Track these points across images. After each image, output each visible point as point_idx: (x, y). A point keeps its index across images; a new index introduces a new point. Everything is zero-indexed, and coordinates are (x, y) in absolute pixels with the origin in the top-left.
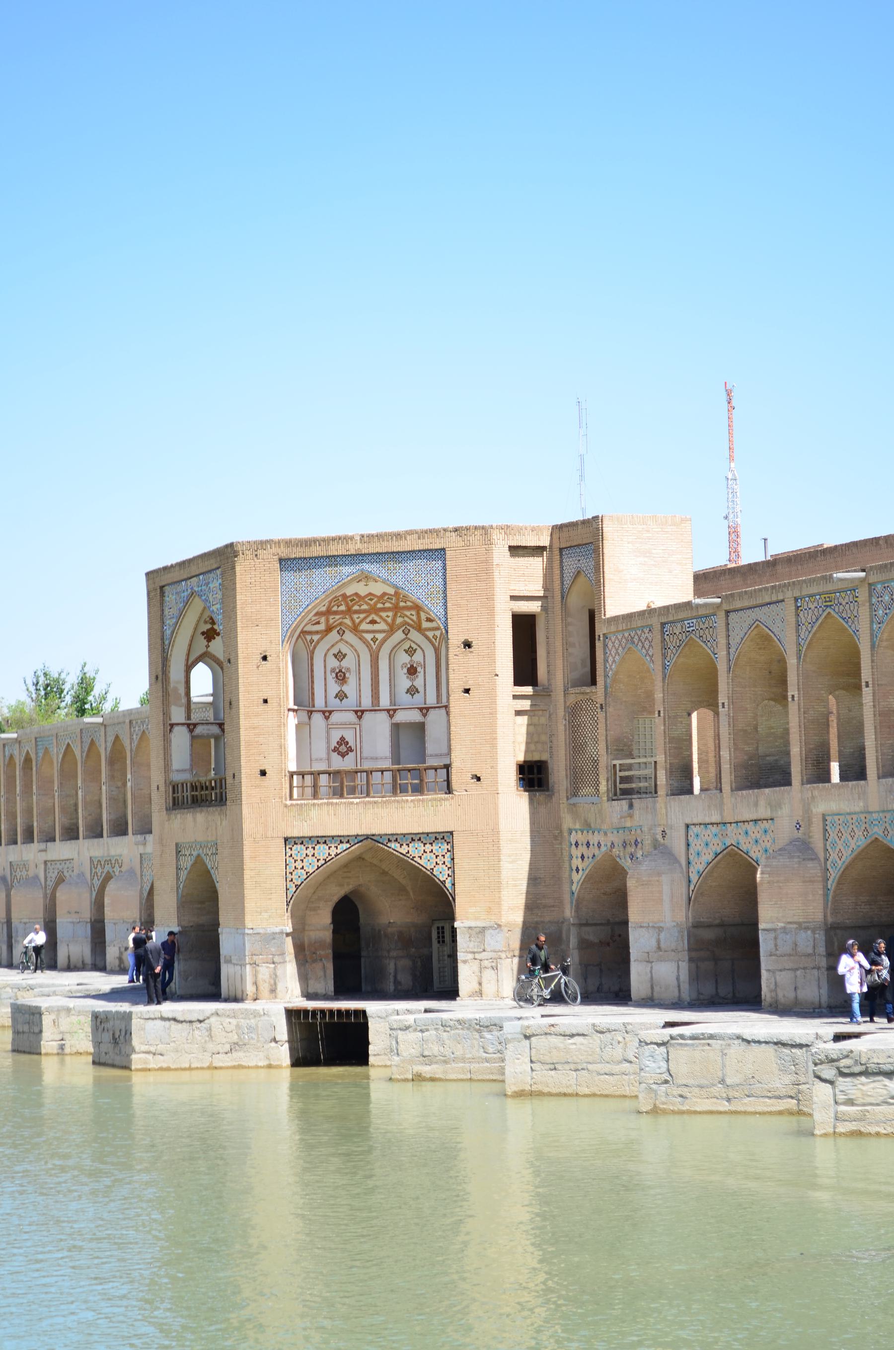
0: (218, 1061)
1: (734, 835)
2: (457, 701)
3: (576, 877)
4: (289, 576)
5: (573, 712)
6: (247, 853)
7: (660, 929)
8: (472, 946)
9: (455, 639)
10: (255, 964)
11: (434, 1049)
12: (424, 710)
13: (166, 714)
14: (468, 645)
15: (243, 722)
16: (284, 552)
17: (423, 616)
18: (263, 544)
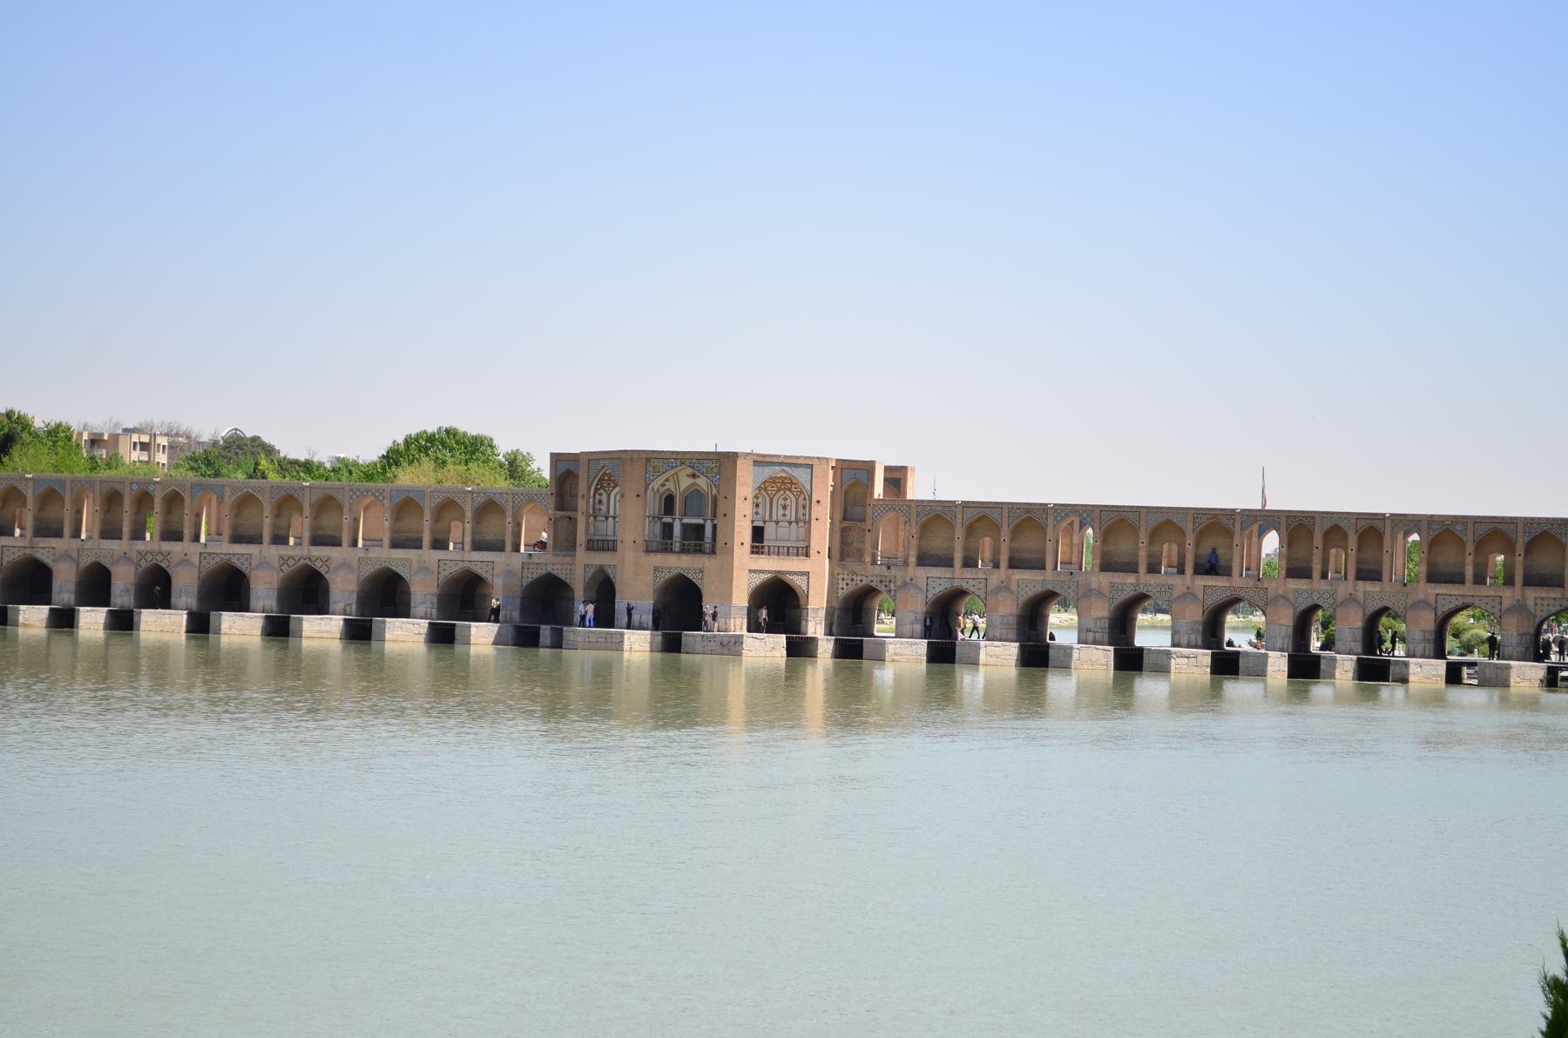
0: (769, 654)
1: (957, 583)
2: (813, 522)
3: (840, 591)
4: (757, 468)
5: (844, 531)
6: (734, 575)
7: (917, 613)
8: (814, 615)
9: (814, 499)
10: (735, 618)
11: (898, 651)
12: (765, 522)
13: (645, 512)
14: (818, 502)
15: (736, 523)
16: (756, 458)
17: (793, 486)
18: (748, 454)
